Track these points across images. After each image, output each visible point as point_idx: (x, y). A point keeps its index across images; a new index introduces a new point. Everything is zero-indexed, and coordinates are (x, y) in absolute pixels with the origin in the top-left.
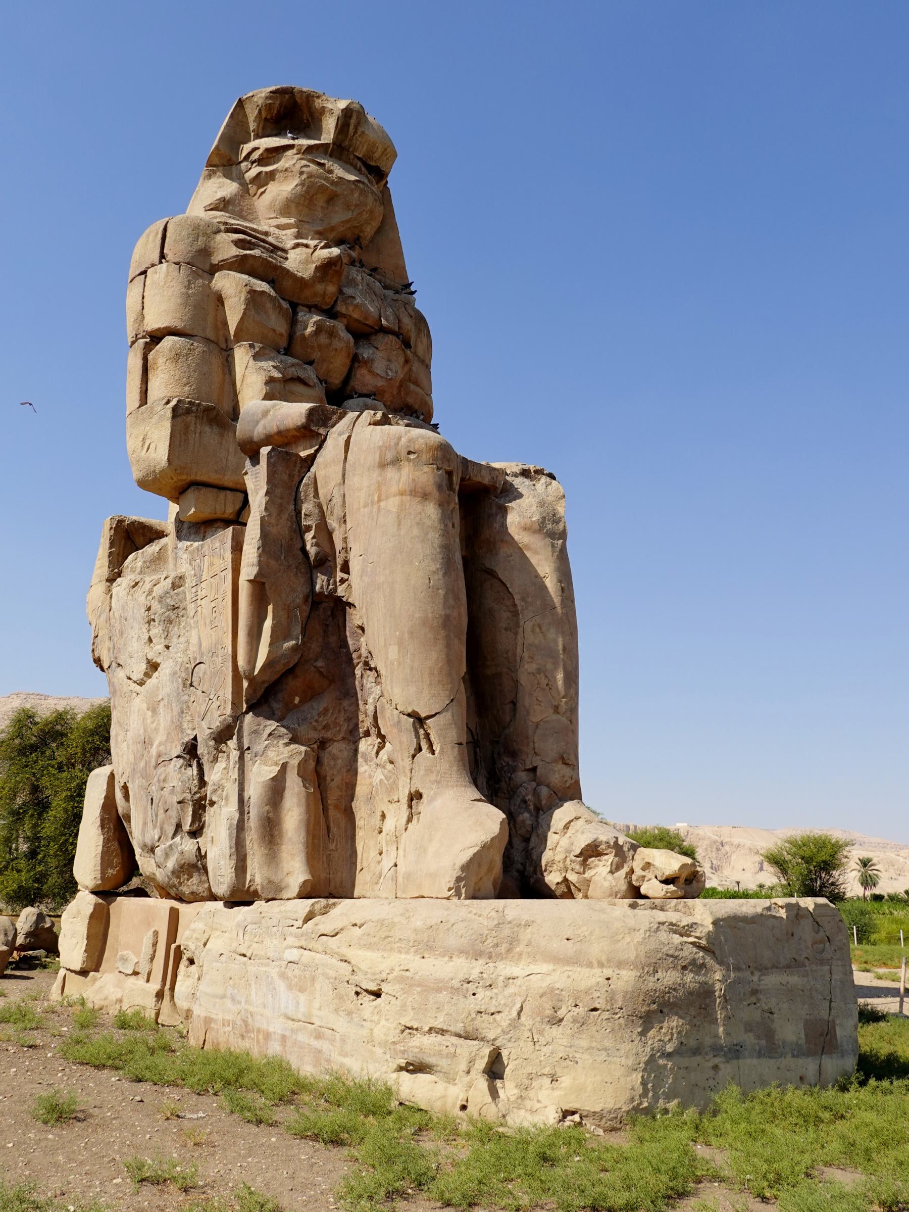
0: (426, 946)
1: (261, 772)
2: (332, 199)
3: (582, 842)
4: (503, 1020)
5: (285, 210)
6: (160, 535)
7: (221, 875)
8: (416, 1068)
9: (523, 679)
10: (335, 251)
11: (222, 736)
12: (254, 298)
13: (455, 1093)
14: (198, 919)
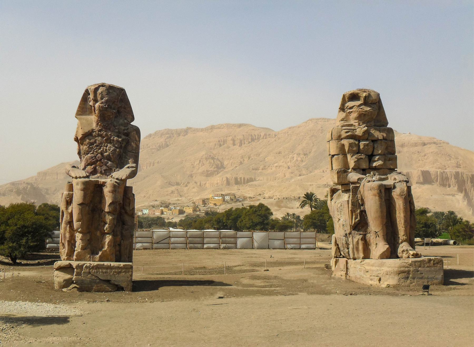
0: (372, 265)
1: (355, 240)
2: (365, 115)
3: (402, 250)
4: (381, 274)
5: (356, 119)
6: (339, 190)
7: (351, 256)
8: (371, 280)
9: (398, 222)
10: (366, 128)
11: (350, 234)
12: (351, 145)
13: (375, 283)
14: (351, 262)
